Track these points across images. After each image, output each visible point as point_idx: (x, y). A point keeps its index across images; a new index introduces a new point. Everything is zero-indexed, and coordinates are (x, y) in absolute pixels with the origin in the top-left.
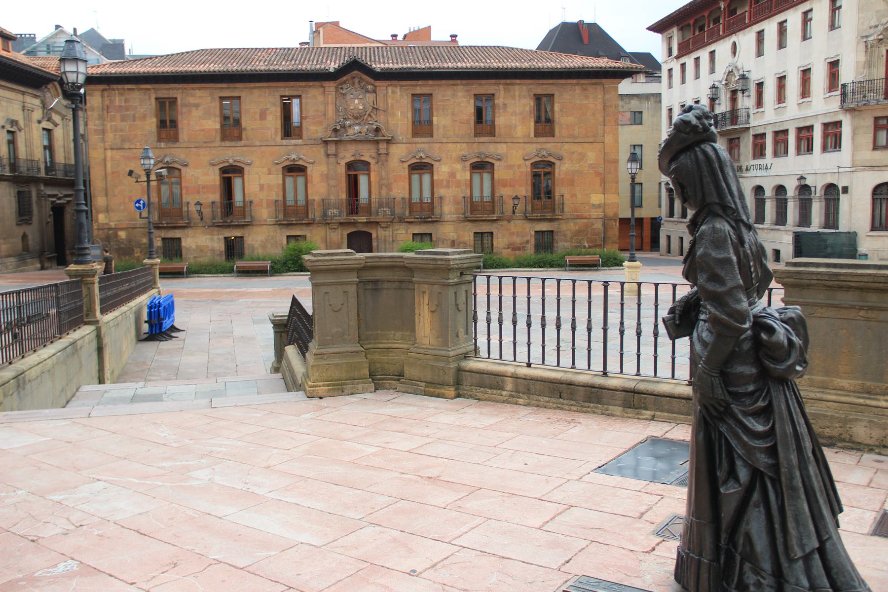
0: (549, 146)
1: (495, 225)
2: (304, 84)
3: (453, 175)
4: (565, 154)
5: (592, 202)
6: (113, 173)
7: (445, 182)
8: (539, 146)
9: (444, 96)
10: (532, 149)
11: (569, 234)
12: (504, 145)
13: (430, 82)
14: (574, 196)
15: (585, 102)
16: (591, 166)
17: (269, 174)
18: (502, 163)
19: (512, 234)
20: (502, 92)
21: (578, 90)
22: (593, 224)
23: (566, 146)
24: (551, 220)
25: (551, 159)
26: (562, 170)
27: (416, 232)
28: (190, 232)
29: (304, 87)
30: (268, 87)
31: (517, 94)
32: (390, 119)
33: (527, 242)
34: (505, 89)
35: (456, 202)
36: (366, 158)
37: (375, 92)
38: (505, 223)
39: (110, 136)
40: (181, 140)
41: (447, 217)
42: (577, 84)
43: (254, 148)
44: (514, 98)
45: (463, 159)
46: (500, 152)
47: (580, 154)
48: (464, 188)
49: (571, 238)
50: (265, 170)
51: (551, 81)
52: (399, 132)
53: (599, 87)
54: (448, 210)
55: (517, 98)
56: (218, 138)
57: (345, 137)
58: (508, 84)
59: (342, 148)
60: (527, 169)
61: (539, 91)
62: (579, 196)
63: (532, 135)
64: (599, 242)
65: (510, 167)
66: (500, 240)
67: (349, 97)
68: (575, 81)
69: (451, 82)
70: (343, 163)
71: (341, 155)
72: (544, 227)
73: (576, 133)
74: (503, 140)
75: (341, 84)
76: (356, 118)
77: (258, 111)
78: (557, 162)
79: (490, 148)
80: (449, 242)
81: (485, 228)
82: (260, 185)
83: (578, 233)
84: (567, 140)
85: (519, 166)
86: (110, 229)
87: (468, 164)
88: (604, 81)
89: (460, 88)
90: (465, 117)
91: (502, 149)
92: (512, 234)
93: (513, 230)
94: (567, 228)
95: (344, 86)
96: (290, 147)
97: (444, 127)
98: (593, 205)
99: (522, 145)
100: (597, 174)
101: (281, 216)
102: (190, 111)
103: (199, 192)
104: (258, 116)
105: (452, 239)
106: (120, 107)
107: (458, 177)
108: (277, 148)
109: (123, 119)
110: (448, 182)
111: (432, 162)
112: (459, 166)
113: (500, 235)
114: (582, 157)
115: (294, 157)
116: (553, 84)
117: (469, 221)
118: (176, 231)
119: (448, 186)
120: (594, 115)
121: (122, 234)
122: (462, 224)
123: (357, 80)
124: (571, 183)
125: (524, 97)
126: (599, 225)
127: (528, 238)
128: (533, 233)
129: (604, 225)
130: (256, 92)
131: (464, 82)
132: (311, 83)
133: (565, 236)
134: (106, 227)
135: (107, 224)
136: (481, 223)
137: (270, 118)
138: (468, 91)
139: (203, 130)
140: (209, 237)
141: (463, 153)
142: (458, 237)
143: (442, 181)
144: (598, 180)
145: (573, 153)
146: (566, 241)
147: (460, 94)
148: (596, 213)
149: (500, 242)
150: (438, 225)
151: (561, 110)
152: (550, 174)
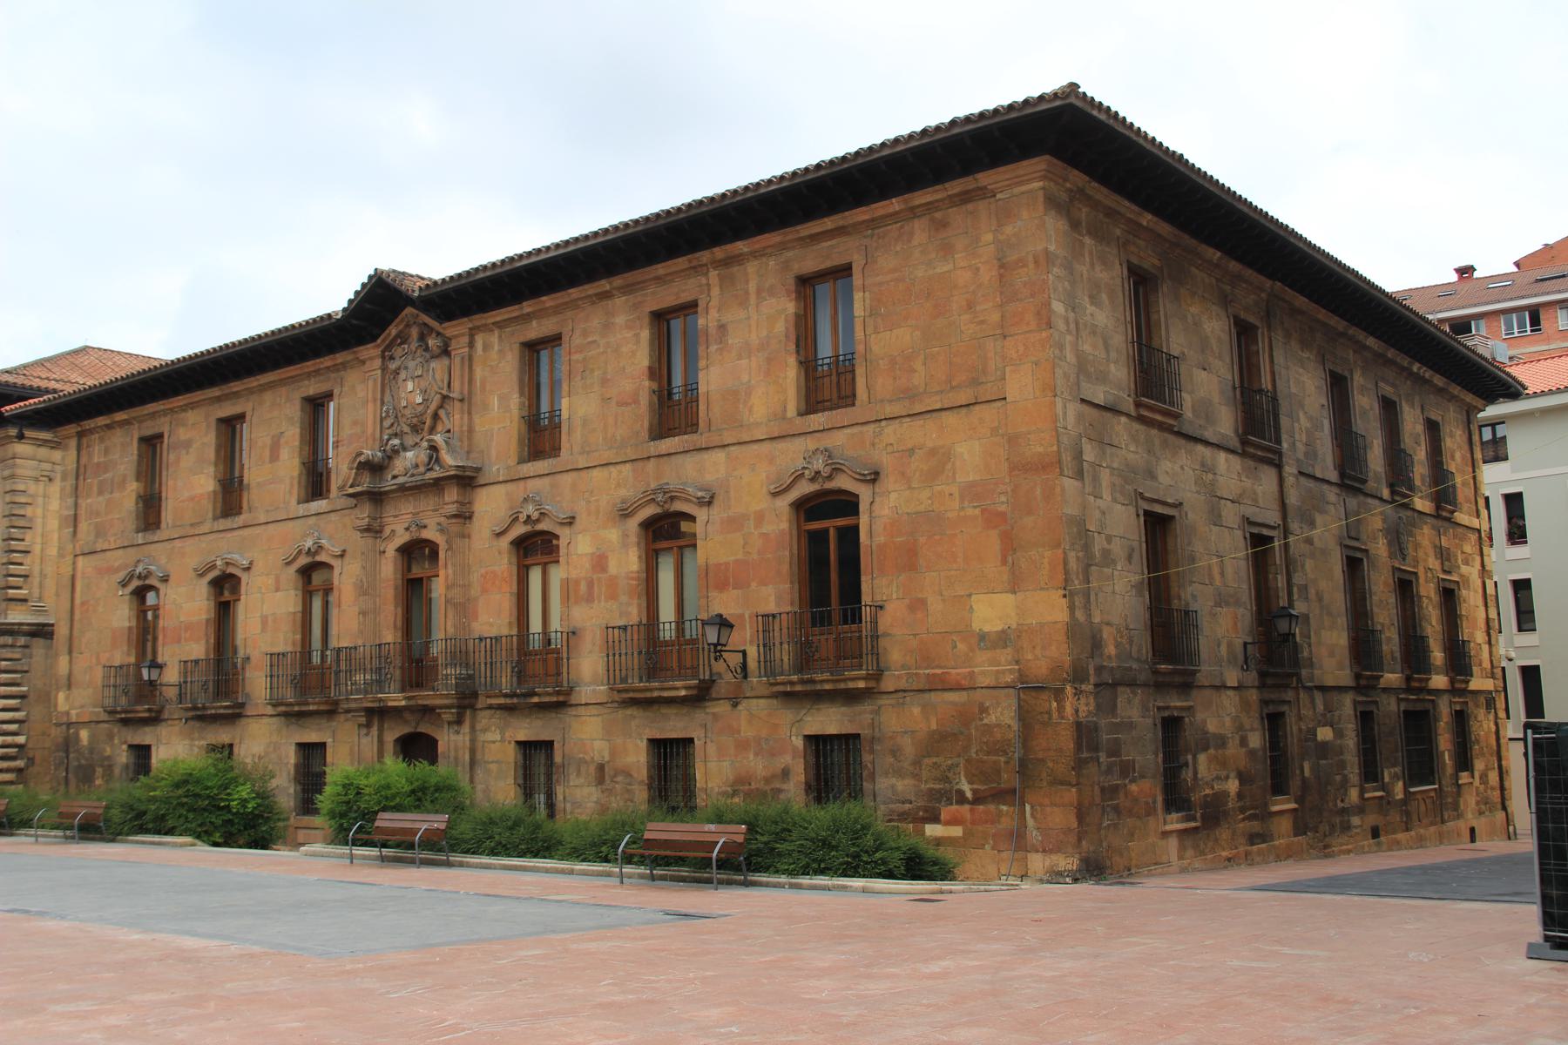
0: (838, 440)
1: (700, 715)
2: (326, 362)
3: (600, 562)
4: (886, 461)
5: (976, 626)
6: (83, 604)
7: (583, 587)
8: (810, 443)
9: (585, 334)
10: (792, 455)
11: (909, 747)
12: (719, 456)
13: (548, 301)
14: (918, 605)
15: (942, 268)
16: (972, 492)
17: (277, 590)
18: (716, 512)
19: (742, 746)
20: (715, 291)
21: (919, 231)
22: (983, 710)
23: (890, 431)
24: (851, 697)
25: (843, 482)
26: (879, 518)
27: (522, 738)
28: (163, 730)
29: (335, 368)
30: (283, 382)
31: (752, 286)
32: (477, 419)
33: (786, 774)
34: (721, 278)
35: (610, 649)
36: (430, 534)
37: (446, 352)
38: (722, 708)
39: (83, 526)
40: (163, 525)
41: (585, 693)
42: (913, 213)
43: (258, 530)
44: (743, 303)
45: (625, 514)
46: (709, 478)
47: (933, 452)
48: (624, 598)
49: (917, 763)
50: (271, 581)
51: (828, 223)
52: (494, 453)
53: (982, 206)
54: (589, 669)
55: (753, 299)
56: (210, 515)
57: (388, 484)
58: (727, 262)
59: (389, 510)
60: (779, 521)
61: (811, 261)
62: (935, 604)
63: (791, 411)
64: (1009, 779)
65: (734, 523)
66: (712, 765)
67: (403, 375)
68: (895, 204)
69: (590, 289)
70: (391, 548)
71: (387, 531)
72: (829, 720)
73: (918, 379)
74: (716, 440)
75: (389, 347)
76: (416, 429)
77: (268, 441)
78: (865, 493)
79: (690, 470)
80: (592, 769)
81: (674, 726)
82: (267, 619)
83: (937, 742)
84: (890, 410)
85: (760, 518)
86: (69, 725)
87: (633, 524)
88: (985, 178)
89: (619, 301)
90: (627, 386)
91: (711, 468)
92: (742, 746)
93: (747, 732)
94: (901, 723)
95: (398, 352)
96: (312, 520)
97: (585, 422)
98: (983, 637)
99: (765, 447)
100: (993, 518)
101: (289, 695)
102: (178, 459)
103: (179, 641)
104: (267, 453)
105: (597, 758)
106: (98, 464)
107: (613, 568)
108: (290, 524)
109: (100, 493)
110: (590, 584)
111: (558, 530)
112: (613, 535)
113: (712, 749)
114: (940, 461)
115: (309, 543)
116: (841, 231)
117: (634, 702)
118: (147, 729)
119: (590, 599)
120: (970, 306)
121: (84, 734)
122: (621, 713)
123: (414, 332)
124: (909, 559)
125: (771, 292)
126: (1003, 714)
127: (786, 759)
128: (799, 743)
129: (1024, 715)
130: (268, 396)
131: (618, 281)
132: (341, 357)
133: (895, 752)
134: (65, 719)
135: (68, 714)
136: (664, 710)
137: (285, 454)
138: (636, 306)
139: (192, 499)
140: (187, 742)
141: (623, 492)
142: (613, 753)
143: (577, 582)
144: (993, 541)
145: (911, 451)
146: (899, 773)
147: (620, 320)
148: (989, 667)
149: (713, 772)
150: (568, 716)
151: (873, 313)
152: (850, 537)
